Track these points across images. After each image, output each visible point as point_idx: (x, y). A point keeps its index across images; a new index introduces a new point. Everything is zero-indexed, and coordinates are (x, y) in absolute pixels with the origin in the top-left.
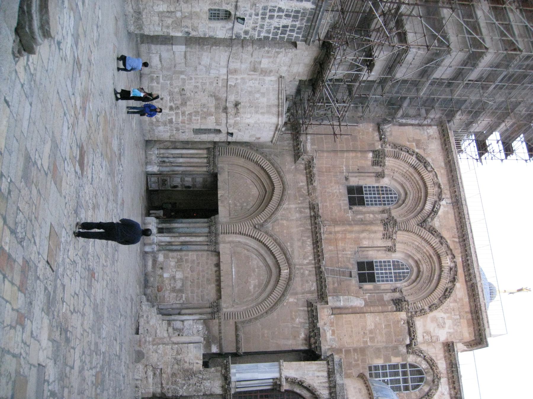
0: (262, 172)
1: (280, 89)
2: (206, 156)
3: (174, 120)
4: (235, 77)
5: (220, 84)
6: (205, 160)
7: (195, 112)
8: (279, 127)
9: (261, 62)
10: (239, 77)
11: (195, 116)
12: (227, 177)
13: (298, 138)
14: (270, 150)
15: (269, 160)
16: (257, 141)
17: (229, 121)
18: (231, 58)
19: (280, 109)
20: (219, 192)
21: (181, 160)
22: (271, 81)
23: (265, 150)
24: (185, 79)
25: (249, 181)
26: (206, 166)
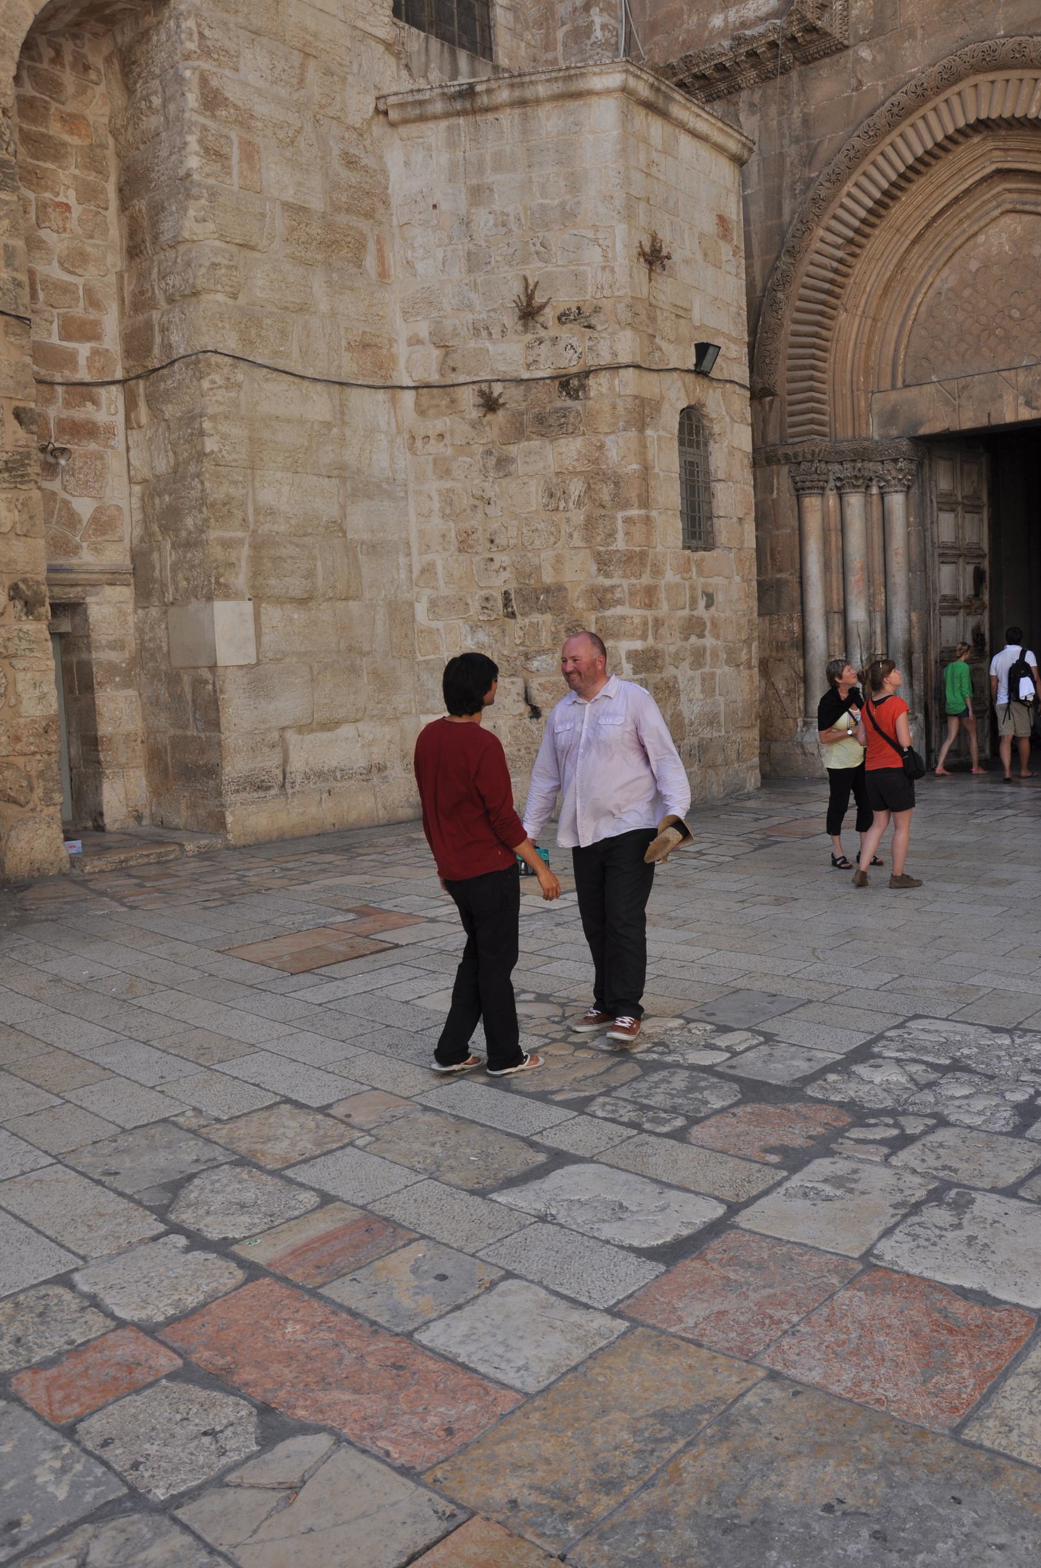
0: (897, 212)
1: (439, 107)
2: (832, 501)
3: (638, 645)
4: (401, 349)
5: (440, 424)
6: (855, 501)
7: (588, 539)
8: (644, 91)
9: (287, 206)
10: (402, 330)
11: (611, 535)
12: (927, 388)
13: (721, 68)
14: (786, 194)
15: (838, 180)
16: (738, 238)
17: (624, 358)
18: (281, 364)
19: (542, 90)
20: (1009, 418)
21: (858, 613)
22: (407, 164)
23: (786, 217)
24: (433, 604)
25: (948, 278)
26: (882, 496)
